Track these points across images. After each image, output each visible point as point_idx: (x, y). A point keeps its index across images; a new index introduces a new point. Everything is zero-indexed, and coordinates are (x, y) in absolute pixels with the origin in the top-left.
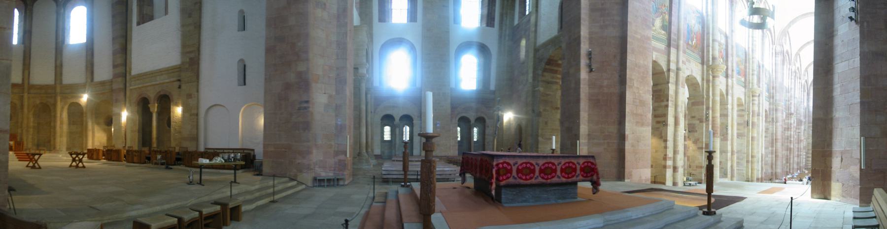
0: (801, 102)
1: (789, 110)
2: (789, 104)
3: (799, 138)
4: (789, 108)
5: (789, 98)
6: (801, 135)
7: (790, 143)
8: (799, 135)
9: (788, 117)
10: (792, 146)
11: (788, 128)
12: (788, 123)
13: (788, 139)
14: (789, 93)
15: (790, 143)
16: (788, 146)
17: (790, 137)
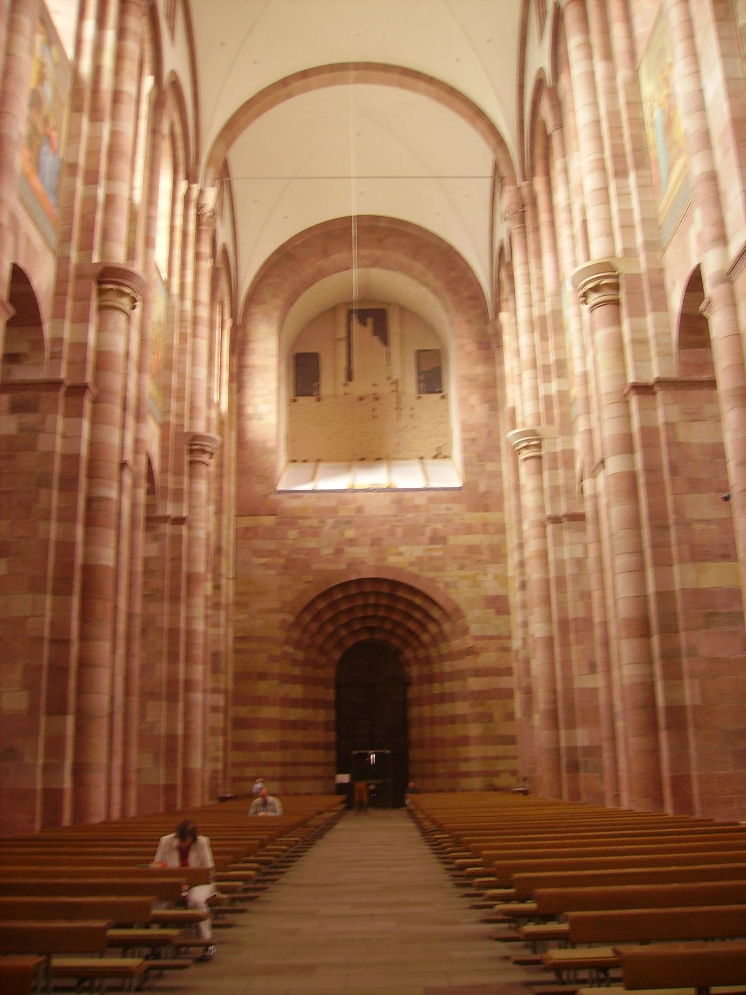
0: (195, 321)
1: (86, 246)
2: (90, 201)
3: (177, 559)
4: (88, 228)
5: (93, 153)
6: (191, 541)
7: (90, 522)
8: (177, 539)
9: (82, 299)
10: (107, 557)
11: (78, 390)
12: (80, 347)
13: (69, 484)
14: (96, 116)
15: (90, 522)
16: (66, 547)
17: (93, 473)
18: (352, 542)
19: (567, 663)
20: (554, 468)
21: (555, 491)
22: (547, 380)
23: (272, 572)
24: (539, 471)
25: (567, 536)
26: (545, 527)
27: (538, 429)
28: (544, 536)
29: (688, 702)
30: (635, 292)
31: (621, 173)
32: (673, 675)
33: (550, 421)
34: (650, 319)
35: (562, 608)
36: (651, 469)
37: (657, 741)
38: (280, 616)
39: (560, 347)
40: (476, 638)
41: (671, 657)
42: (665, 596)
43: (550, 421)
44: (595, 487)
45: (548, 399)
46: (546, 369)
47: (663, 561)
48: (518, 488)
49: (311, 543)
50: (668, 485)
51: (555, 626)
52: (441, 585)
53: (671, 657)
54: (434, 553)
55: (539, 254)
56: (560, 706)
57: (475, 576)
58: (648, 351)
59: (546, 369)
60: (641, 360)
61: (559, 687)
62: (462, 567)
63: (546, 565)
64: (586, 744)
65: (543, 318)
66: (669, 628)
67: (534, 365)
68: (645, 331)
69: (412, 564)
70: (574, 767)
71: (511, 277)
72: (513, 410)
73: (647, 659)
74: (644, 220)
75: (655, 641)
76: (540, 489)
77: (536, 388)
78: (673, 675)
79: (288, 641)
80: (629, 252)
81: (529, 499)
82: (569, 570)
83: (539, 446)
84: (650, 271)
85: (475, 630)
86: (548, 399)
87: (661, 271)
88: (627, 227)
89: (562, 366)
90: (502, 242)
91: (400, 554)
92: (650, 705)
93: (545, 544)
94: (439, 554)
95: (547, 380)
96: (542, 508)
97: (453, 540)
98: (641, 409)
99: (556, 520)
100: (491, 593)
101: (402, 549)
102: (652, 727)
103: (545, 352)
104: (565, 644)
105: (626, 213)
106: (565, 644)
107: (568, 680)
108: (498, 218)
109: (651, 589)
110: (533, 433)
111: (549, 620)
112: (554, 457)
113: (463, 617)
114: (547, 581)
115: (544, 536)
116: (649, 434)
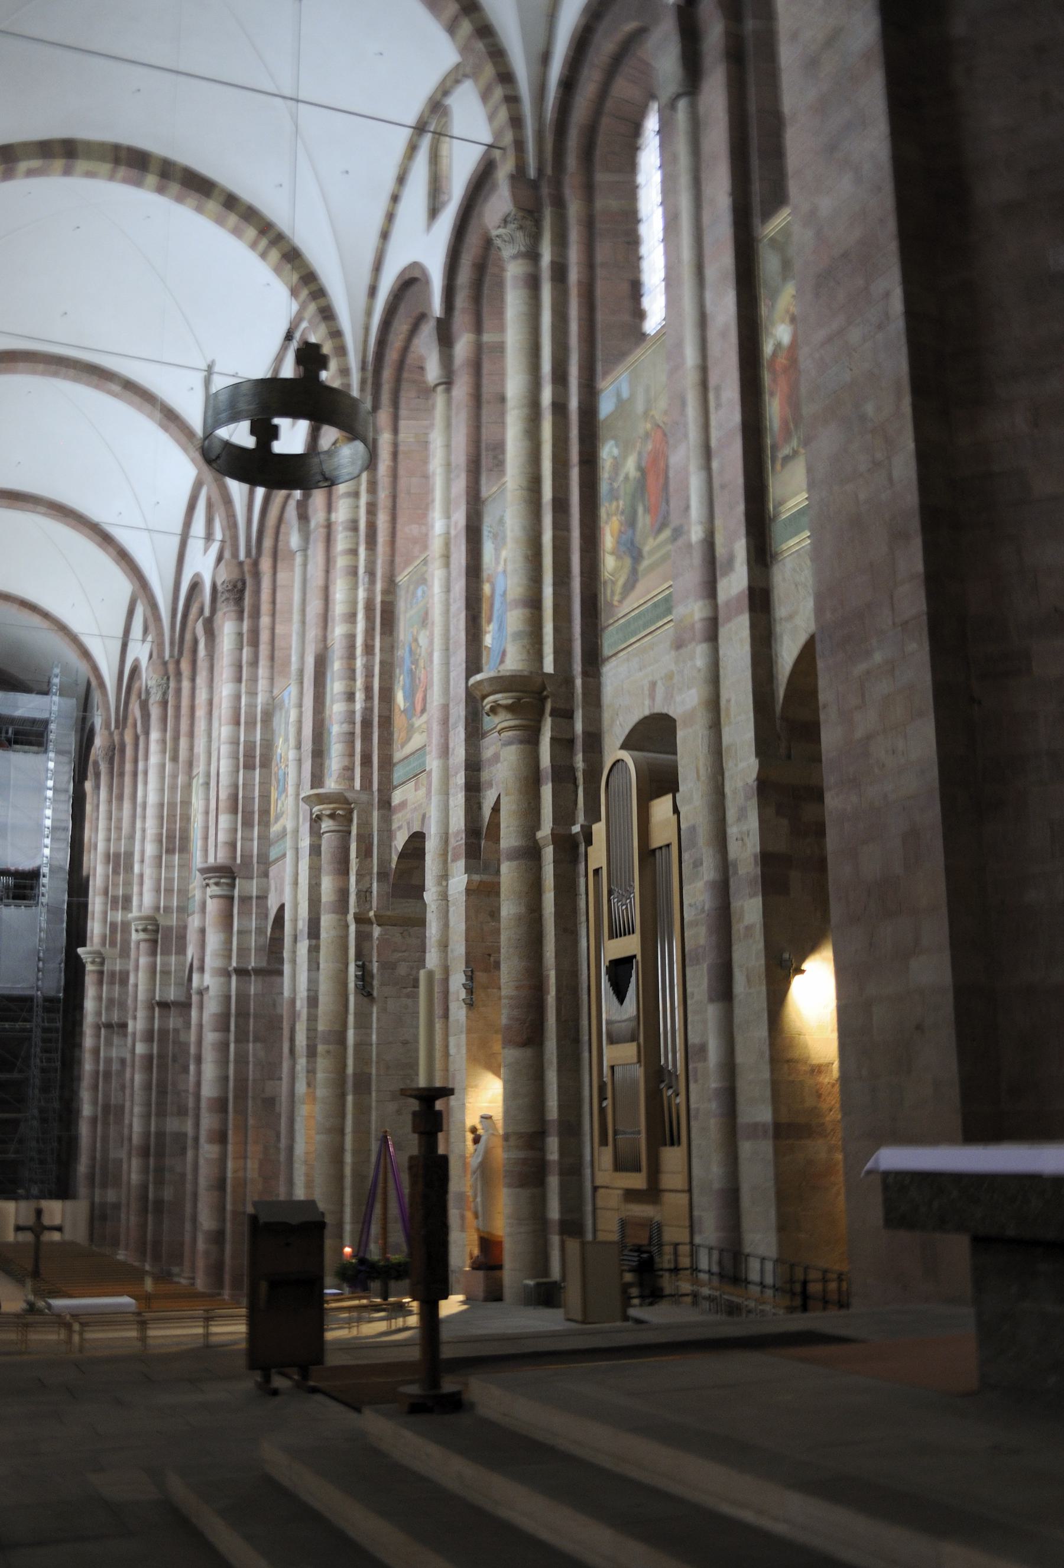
19: (105, 1139)
20: (112, 983)
21: (111, 1001)
22: (114, 908)
24: (100, 983)
25: (116, 1040)
26: (100, 1028)
27: (102, 950)
28: (98, 1036)
29: (166, 1198)
30: (167, 937)
31: (170, 851)
32: (160, 1182)
33: (113, 944)
34: (173, 959)
35: (107, 1096)
36: (162, 1056)
37: (146, 1220)
39: (128, 884)
41: (160, 1171)
42: (161, 1135)
43: (113, 944)
44: (135, 1028)
45: (113, 926)
46: (115, 900)
47: (162, 1113)
50: (170, 1067)
51: (99, 1109)
53: (160, 1171)
56: (97, 1170)
58: (170, 979)
59: (115, 900)
60: (165, 984)
61: (98, 1155)
65: (117, 855)
66: (160, 1155)
67: (106, 892)
68: (170, 965)
70: (104, 1218)
73: (145, 1170)
74: (179, 891)
75: (152, 1161)
76: (99, 998)
77: (105, 913)
78: (160, 1182)
80: (168, 909)
81: (89, 1005)
82: (115, 1067)
83: (102, 963)
84: (178, 927)
86: (113, 926)
87: (185, 927)
88: (169, 891)
89: (127, 900)
92: (144, 1198)
93: (100, 1043)
95: (114, 908)
96: (99, 1014)
98: (160, 1017)
99: (109, 1026)
102: (144, 1211)
103: (116, 885)
104: (106, 1124)
105: (169, 880)
106: (106, 1124)
107: (105, 1151)
109: (153, 1129)
110: (99, 954)
111: (95, 1102)
112: (113, 974)
114: (97, 1072)
115: (98, 1036)
116: (164, 1032)
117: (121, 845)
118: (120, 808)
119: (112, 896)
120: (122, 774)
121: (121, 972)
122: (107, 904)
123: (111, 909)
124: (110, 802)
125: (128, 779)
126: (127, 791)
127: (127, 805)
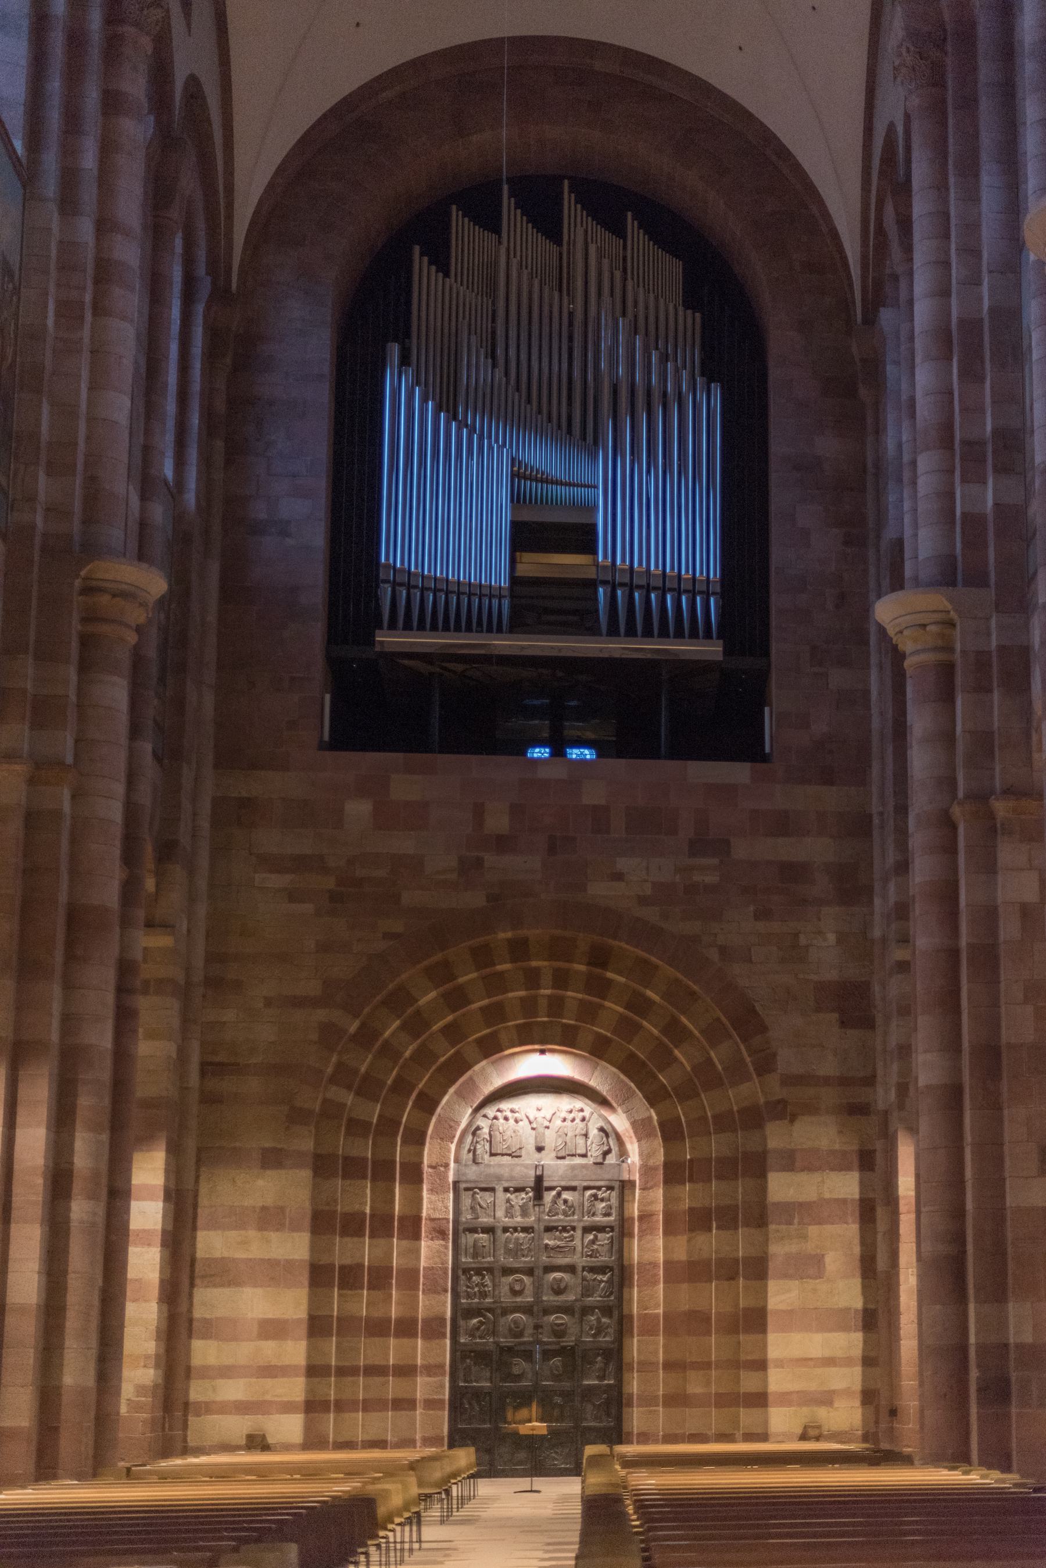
18: (502, 843)
20: (982, 688)
22: (974, 475)
23: (308, 908)
24: (946, 695)
38: (321, 1015)
40: (791, 1080)
45: (974, 523)
46: (973, 451)
48: (900, 730)
49: (404, 844)
52: (714, 954)
54: (697, 878)
55: (970, 169)
57: (796, 935)
59: (973, 451)
62: (763, 914)
63: (953, 915)
64: (1028, 1338)
65: (971, 326)
69: (643, 901)
71: (905, 224)
72: (900, 543)
76: (948, 737)
79: (343, 1076)
85: (787, 1060)
90: (891, 127)
91: (618, 877)
94: (711, 879)
97: (741, 850)
100: (831, 975)
101: (623, 864)
108: (885, 70)
111: (952, 1045)
113: (763, 1029)
117: (980, 299)
118: (972, 197)
119: (964, 442)
120: (969, 104)
121: (1001, 648)
122: (951, 471)
123: (964, 480)
124: (941, 187)
125: (987, 108)
126: (988, 139)
127: (989, 180)
